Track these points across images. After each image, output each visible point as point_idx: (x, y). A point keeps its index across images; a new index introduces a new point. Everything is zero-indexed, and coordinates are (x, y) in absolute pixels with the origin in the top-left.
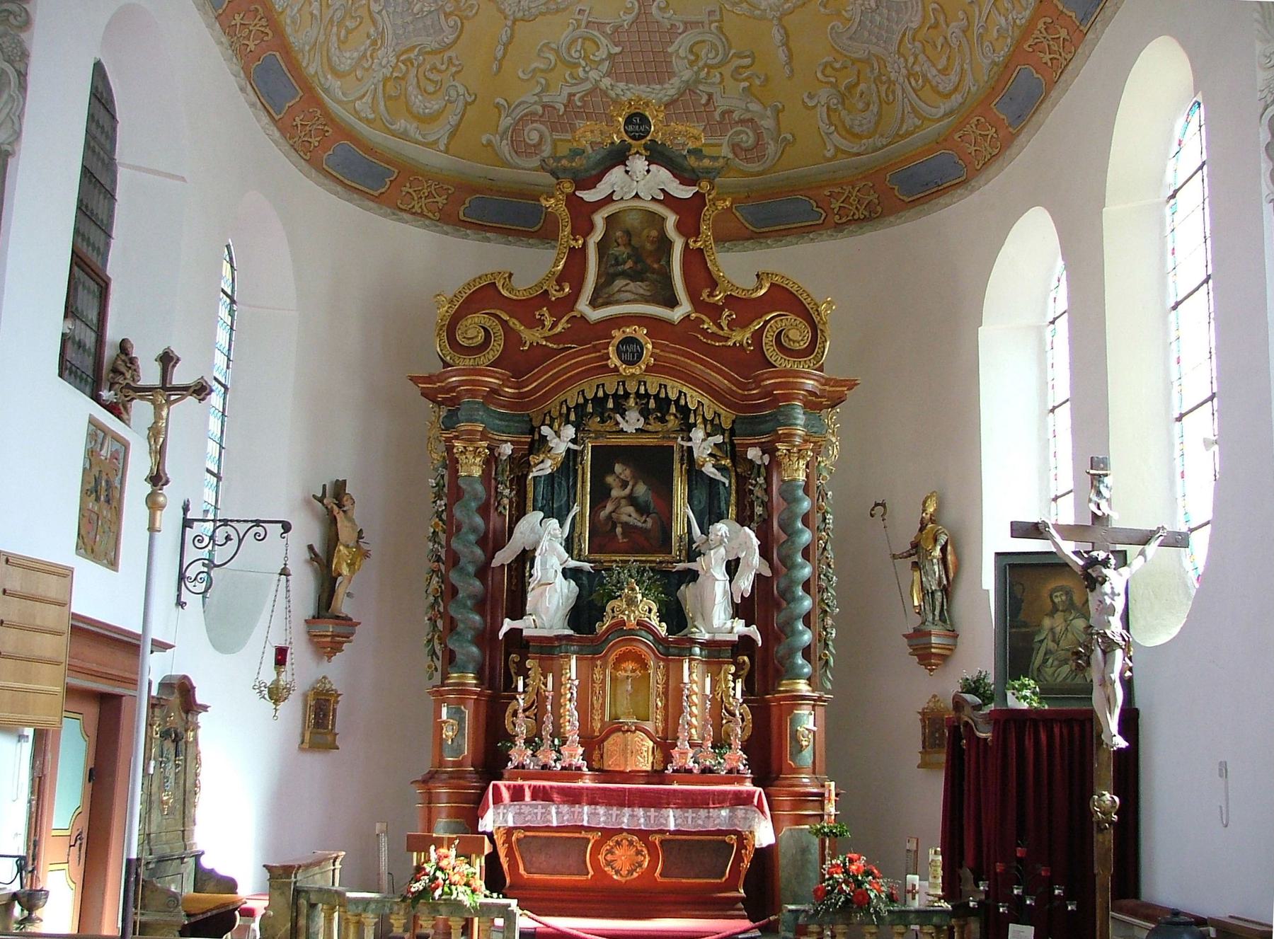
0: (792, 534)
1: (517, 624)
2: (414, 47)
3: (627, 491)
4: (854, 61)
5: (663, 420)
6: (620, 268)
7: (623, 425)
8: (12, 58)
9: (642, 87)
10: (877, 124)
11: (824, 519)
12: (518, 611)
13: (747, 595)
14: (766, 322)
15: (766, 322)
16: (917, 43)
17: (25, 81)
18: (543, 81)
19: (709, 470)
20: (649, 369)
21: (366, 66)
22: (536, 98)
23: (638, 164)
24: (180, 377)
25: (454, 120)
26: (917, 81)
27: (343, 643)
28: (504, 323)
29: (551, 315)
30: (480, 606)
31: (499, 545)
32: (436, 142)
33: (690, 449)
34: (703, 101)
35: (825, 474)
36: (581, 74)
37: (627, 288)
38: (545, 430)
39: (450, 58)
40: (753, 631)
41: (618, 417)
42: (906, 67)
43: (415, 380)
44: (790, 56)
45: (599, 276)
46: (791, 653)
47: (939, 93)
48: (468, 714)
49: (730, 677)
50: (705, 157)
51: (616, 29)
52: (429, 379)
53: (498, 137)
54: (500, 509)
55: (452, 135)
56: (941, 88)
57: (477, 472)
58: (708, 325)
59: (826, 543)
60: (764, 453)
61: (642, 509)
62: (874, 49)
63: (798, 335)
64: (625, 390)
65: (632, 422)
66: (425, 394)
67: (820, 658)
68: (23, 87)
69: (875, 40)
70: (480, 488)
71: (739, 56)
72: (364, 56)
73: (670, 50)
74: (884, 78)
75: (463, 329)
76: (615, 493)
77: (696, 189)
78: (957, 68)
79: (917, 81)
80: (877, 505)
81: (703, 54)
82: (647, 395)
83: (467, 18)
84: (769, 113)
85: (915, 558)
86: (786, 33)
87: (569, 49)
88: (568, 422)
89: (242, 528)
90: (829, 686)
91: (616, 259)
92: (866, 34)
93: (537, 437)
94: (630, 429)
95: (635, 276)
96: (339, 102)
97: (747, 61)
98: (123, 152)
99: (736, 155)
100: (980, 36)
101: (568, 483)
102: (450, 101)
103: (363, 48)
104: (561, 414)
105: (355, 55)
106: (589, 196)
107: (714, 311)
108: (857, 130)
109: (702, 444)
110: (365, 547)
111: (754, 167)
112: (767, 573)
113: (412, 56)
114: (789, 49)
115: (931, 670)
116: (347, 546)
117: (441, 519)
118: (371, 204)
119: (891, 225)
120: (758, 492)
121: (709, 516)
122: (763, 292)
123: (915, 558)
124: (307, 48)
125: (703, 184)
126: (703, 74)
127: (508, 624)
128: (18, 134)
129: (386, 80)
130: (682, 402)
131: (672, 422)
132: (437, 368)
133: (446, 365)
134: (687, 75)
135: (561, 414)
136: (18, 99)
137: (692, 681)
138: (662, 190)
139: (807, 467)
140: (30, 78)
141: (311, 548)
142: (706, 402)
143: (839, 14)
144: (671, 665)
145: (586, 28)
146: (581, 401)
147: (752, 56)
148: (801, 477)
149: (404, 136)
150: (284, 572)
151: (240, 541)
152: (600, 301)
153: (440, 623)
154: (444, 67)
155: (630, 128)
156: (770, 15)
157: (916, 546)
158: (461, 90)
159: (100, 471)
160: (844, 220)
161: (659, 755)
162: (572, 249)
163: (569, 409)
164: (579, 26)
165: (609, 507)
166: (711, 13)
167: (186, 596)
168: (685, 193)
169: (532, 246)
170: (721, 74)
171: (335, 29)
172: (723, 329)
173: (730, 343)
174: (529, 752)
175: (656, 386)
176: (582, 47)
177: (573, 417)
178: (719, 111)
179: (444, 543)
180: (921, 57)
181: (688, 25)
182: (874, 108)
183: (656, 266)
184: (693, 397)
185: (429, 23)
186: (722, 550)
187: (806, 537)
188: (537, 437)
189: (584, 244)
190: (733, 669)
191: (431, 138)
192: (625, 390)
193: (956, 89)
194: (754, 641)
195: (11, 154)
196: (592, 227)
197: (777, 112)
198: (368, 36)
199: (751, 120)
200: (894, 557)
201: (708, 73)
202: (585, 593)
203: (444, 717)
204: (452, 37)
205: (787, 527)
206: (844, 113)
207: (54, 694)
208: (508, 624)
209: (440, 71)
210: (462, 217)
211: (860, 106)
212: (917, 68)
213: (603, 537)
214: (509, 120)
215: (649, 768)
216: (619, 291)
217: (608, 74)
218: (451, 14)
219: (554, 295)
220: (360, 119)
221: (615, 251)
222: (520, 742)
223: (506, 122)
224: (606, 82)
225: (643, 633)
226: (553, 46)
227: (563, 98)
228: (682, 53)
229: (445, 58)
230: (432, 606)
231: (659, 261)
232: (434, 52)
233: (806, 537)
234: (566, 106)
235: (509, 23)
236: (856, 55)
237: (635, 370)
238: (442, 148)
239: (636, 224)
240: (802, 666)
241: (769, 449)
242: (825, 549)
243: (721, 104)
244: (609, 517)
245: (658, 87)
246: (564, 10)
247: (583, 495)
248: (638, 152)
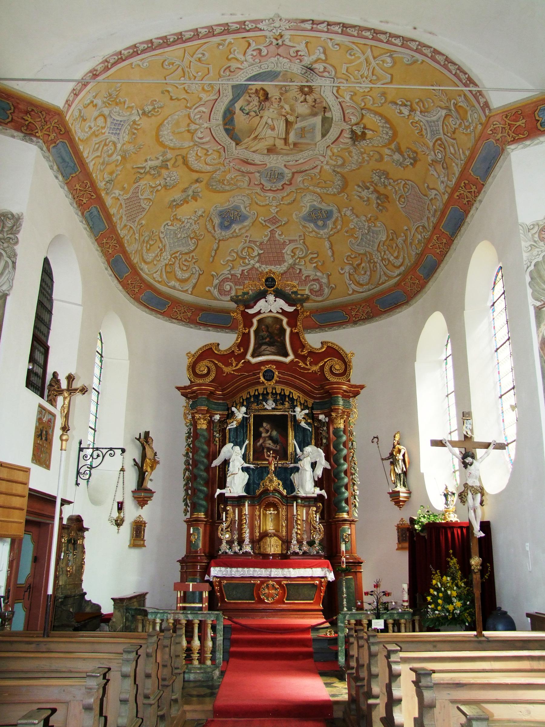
0: (339, 451)
1: (223, 491)
2: (178, 252)
3: (269, 434)
4: (359, 254)
5: (283, 404)
6: (264, 341)
7: (267, 407)
9: (273, 267)
10: (370, 280)
11: (352, 444)
12: (223, 485)
13: (320, 477)
14: (326, 362)
15: (326, 362)
16: (385, 247)
18: (231, 265)
19: (303, 424)
20: (277, 382)
21: (158, 259)
22: (228, 272)
23: (271, 298)
24: (77, 384)
25: (194, 281)
26: (385, 262)
27: (148, 501)
28: (216, 365)
29: (235, 361)
30: (206, 484)
31: (215, 458)
32: (187, 290)
33: (295, 416)
34: (298, 272)
35: (352, 425)
36: (247, 261)
37: (267, 349)
38: (234, 409)
39: (193, 256)
40: (323, 492)
41: (264, 403)
42: (381, 256)
43: (179, 388)
44: (333, 253)
45: (255, 344)
46: (340, 501)
47: (395, 267)
48: (201, 530)
49: (314, 512)
50: (299, 294)
51: (261, 243)
52: (185, 388)
53: (213, 288)
54: (215, 442)
55: (194, 287)
56: (395, 265)
57: (205, 427)
58: (301, 364)
59: (353, 454)
60: (326, 417)
61: (275, 442)
62: (367, 249)
63: (338, 367)
64: (267, 391)
65: (270, 405)
66: (183, 394)
67: (352, 504)
68: (14, 267)
69: (367, 246)
70: (205, 433)
71: (312, 253)
72: (157, 256)
73: (283, 251)
74: (372, 261)
75: (199, 367)
76: (264, 435)
77: (295, 308)
78: (402, 256)
79: (385, 262)
80: (374, 438)
81: (297, 253)
82: (276, 394)
83: (200, 240)
84: (325, 276)
85: (391, 460)
86: (331, 244)
87: (242, 252)
88: (243, 405)
89: (104, 451)
90: (356, 515)
91: (262, 337)
92: (364, 243)
93: (230, 412)
94: (269, 408)
95: (270, 344)
96: (147, 274)
97: (316, 255)
98: (56, 294)
99: (312, 294)
100: (411, 243)
101: (243, 431)
102: (192, 274)
103: (156, 252)
104: (240, 402)
105: (154, 255)
106: (251, 311)
107: (303, 358)
108: (361, 282)
109: (300, 413)
110: (157, 459)
111: (320, 299)
112: (329, 467)
113: (177, 255)
114: (333, 250)
115: (400, 508)
116: (150, 459)
117: (190, 447)
118: (161, 316)
119: (377, 321)
120: (324, 434)
121: (303, 444)
122: (324, 350)
123: (391, 460)
124: (133, 252)
125: (298, 306)
126: (297, 261)
127: (218, 491)
128: (11, 287)
129: (166, 265)
130: (291, 396)
131: (287, 405)
132: (188, 383)
133: (191, 382)
134: (291, 261)
135: (240, 402)
137: (298, 514)
138: (281, 309)
139: (344, 422)
141: (134, 460)
142: (301, 396)
143: (352, 236)
144: (289, 507)
145: (249, 242)
146: (248, 396)
147: (317, 253)
148: (342, 426)
149: (174, 288)
150: (122, 470)
151: (103, 457)
152: (256, 355)
153: (190, 492)
154: (190, 260)
155: (267, 283)
156: (324, 236)
157: (392, 454)
158: (197, 269)
160: (357, 319)
161: (284, 547)
162: (244, 334)
163: (243, 400)
164: (246, 242)
165: (261, 441)
166: (300, 236)
167: (80, 481)
168: (291, 309)
169: (227, 333)
170: (305, 261)
171: (145, 245)
172: (307, 365)
173: (310, 371)
174: (228, 547)
175: (280, 389)
176: (247, 251)
177: (245, 403)
178: (304, 276)
179: (191, 457)
180: (387, 252)
181: (291, 241)
182: (368, 273)
183: (279, 340)
184: (296, 394)
185: (184, 242)
186: (309, 458)
187: (345, 452)
188: (230, 412)
189: (249, 332)
190: (315, 509)
191: (185, 289)
192: (267, 391)
193: (400, 266)
194: (323, 497)
196: (252, 324)
197: (328, 276)
198: (159, 247)
199: (318, 279)
200: (382, 459)
201: (299, 261)
202: (251, 478)
203: (191, 532)
204: (193, 248)
205: (336, 447)
206: (356, 276)
207: (21, 523)
208: (218, 491)
209: (188, 261)
210: (198, 321)
211: (363, 272)
212: (385, 257)
213: (259, 454)
214: (217, 281)
215: (280, 552)
216: (264, 350)
217: (258, 262)
218: (193, 238)
219: (237, 352)
220: (156, 281)
221: (262, 334)
222: (224, 544)
223: (216, 282)
224: (257, 265)
225: (277, 494)
226: (236, 251)
227: (240, 272)
228: (288, 252)
229: (191, 256)
230: (186, 485)
231: (280, 338)
232: (186, 254)
233: (345, 452)
234: (241, 275)
235: (217, 241)
236: (360, 252)
237: (272, 383)
238: (190, 293)
239: (270, 322)
240: (345, 507)
241: (328, 415)
242: (353, 457)
243: (305, 273)
244: (261, 445)
245: (279, 267)
246: (240, 236)
247: (250, 436)
248: (270, 293)
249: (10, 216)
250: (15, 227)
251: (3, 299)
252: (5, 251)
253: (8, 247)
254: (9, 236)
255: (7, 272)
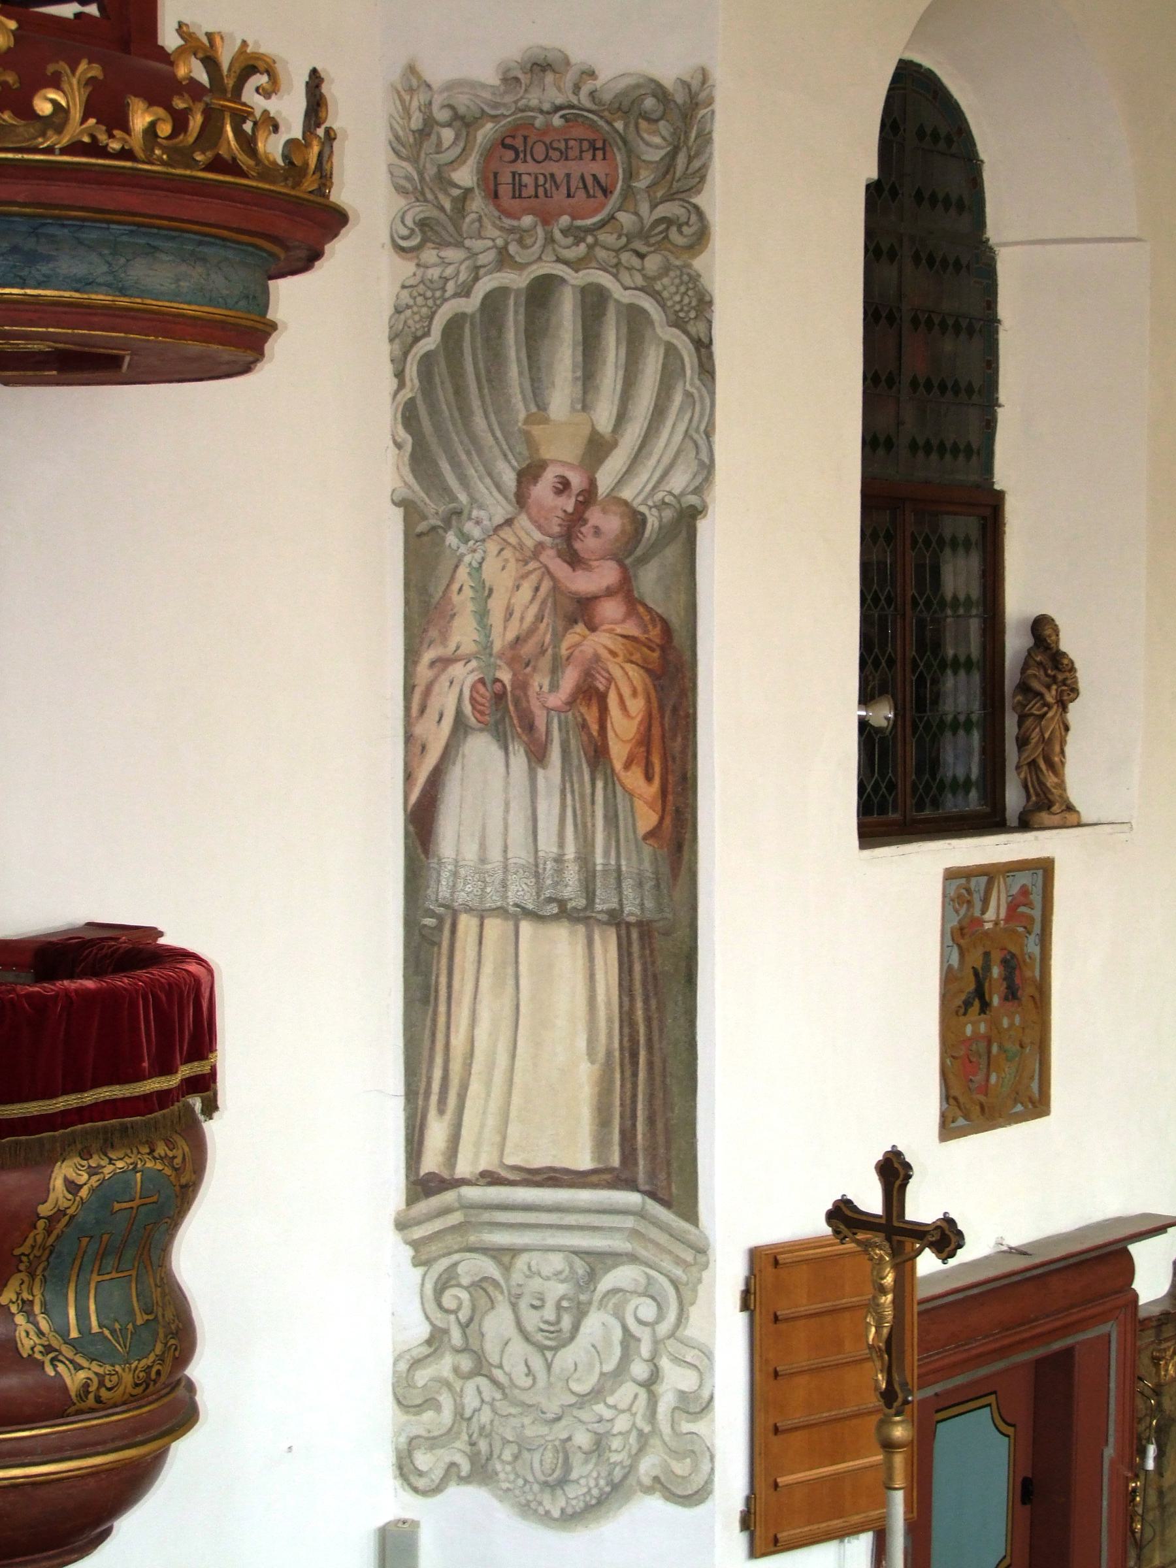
8: (681, 315)
17: (710, 356)
68: (707, 370)
128: (707, 469)
136: (701, 397)
140: (718, 349)
159: (987, 955)
195: (701, 512)
249: (649, 103)
250: (681, 160)
251: (684, 534)
252: (656, 295)
253: (666, 269)
254: (663, 210)
255: (678, 398)
